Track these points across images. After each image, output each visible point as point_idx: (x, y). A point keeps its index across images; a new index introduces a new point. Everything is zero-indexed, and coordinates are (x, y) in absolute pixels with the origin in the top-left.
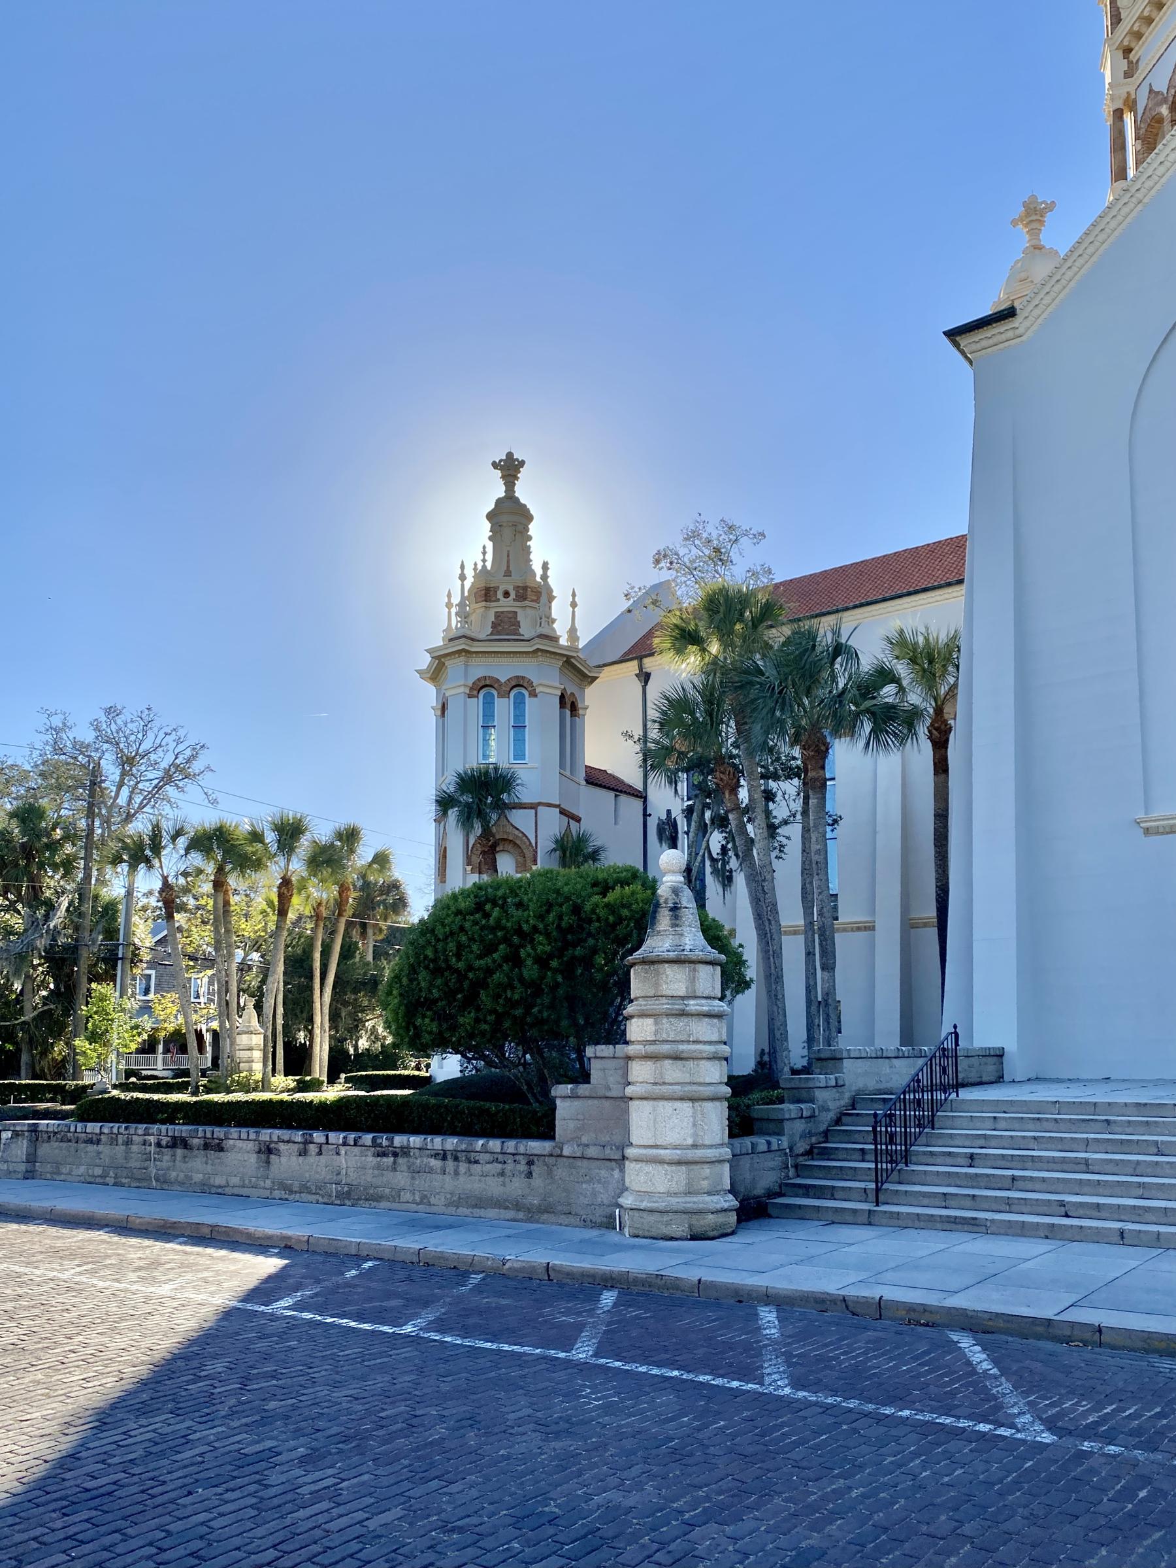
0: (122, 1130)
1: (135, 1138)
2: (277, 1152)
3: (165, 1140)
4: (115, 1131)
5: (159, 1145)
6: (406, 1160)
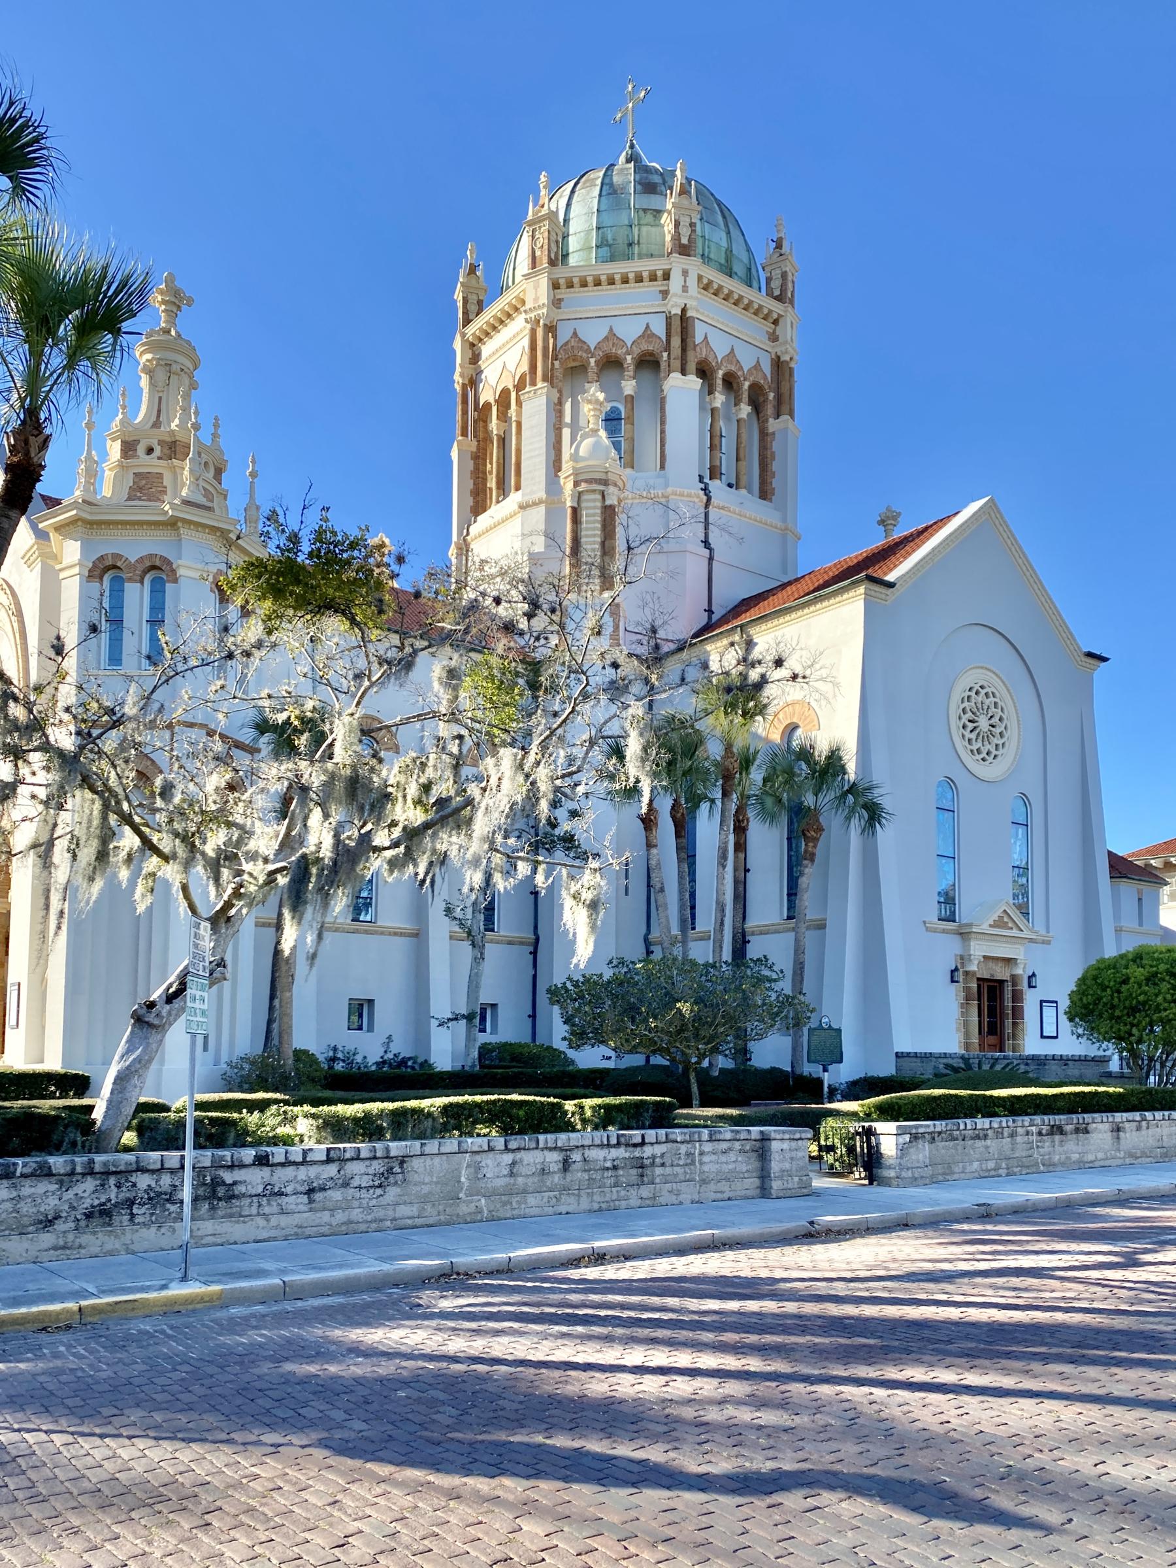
0: (1010, 1123)
1: (1019, 1129)
3: (1045, 1129)
4: (1004, 1124)
5: (1040, 1134)
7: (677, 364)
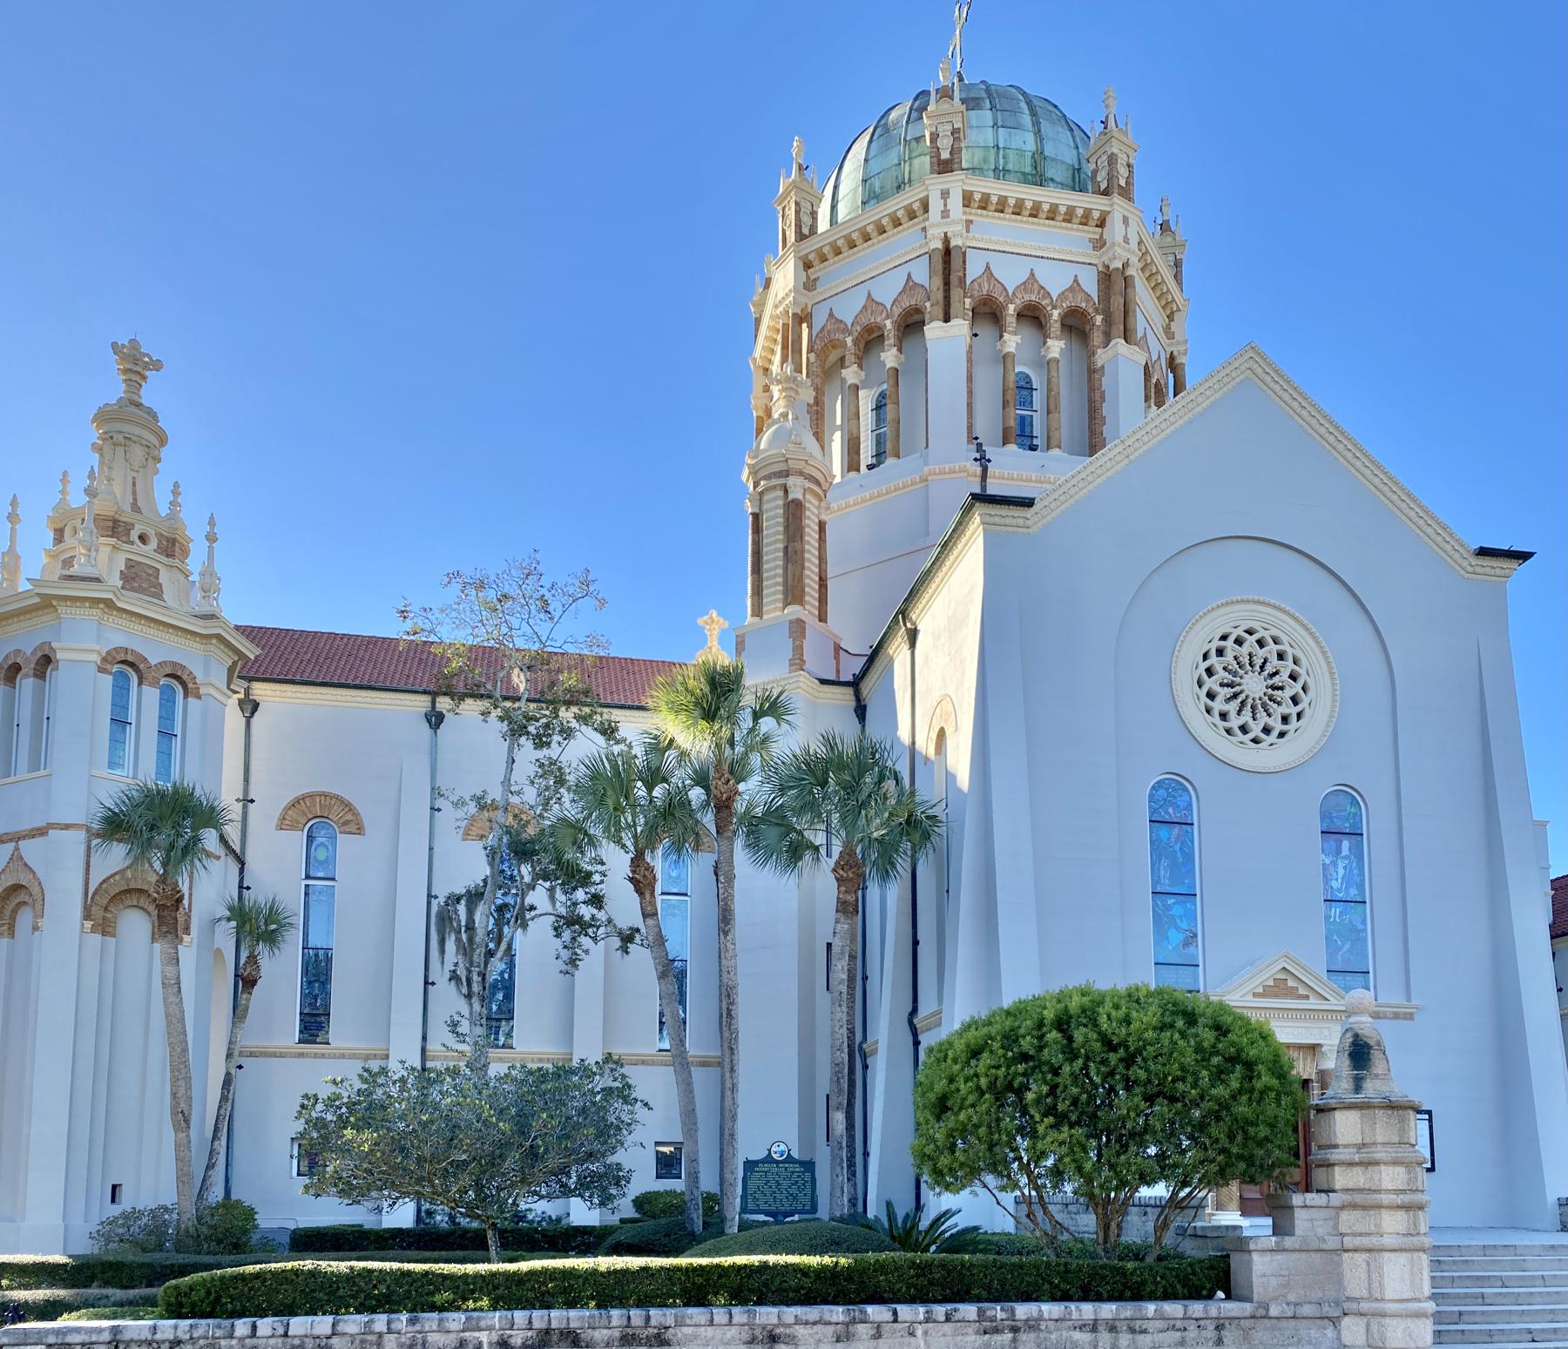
2: (791, 1339)
6: (1032, 1335)
7: (939, 311)
